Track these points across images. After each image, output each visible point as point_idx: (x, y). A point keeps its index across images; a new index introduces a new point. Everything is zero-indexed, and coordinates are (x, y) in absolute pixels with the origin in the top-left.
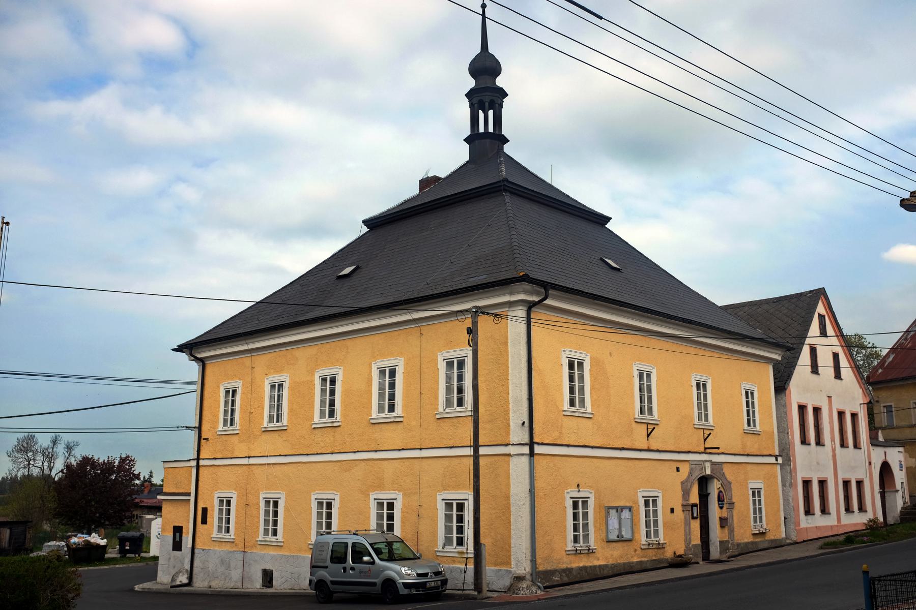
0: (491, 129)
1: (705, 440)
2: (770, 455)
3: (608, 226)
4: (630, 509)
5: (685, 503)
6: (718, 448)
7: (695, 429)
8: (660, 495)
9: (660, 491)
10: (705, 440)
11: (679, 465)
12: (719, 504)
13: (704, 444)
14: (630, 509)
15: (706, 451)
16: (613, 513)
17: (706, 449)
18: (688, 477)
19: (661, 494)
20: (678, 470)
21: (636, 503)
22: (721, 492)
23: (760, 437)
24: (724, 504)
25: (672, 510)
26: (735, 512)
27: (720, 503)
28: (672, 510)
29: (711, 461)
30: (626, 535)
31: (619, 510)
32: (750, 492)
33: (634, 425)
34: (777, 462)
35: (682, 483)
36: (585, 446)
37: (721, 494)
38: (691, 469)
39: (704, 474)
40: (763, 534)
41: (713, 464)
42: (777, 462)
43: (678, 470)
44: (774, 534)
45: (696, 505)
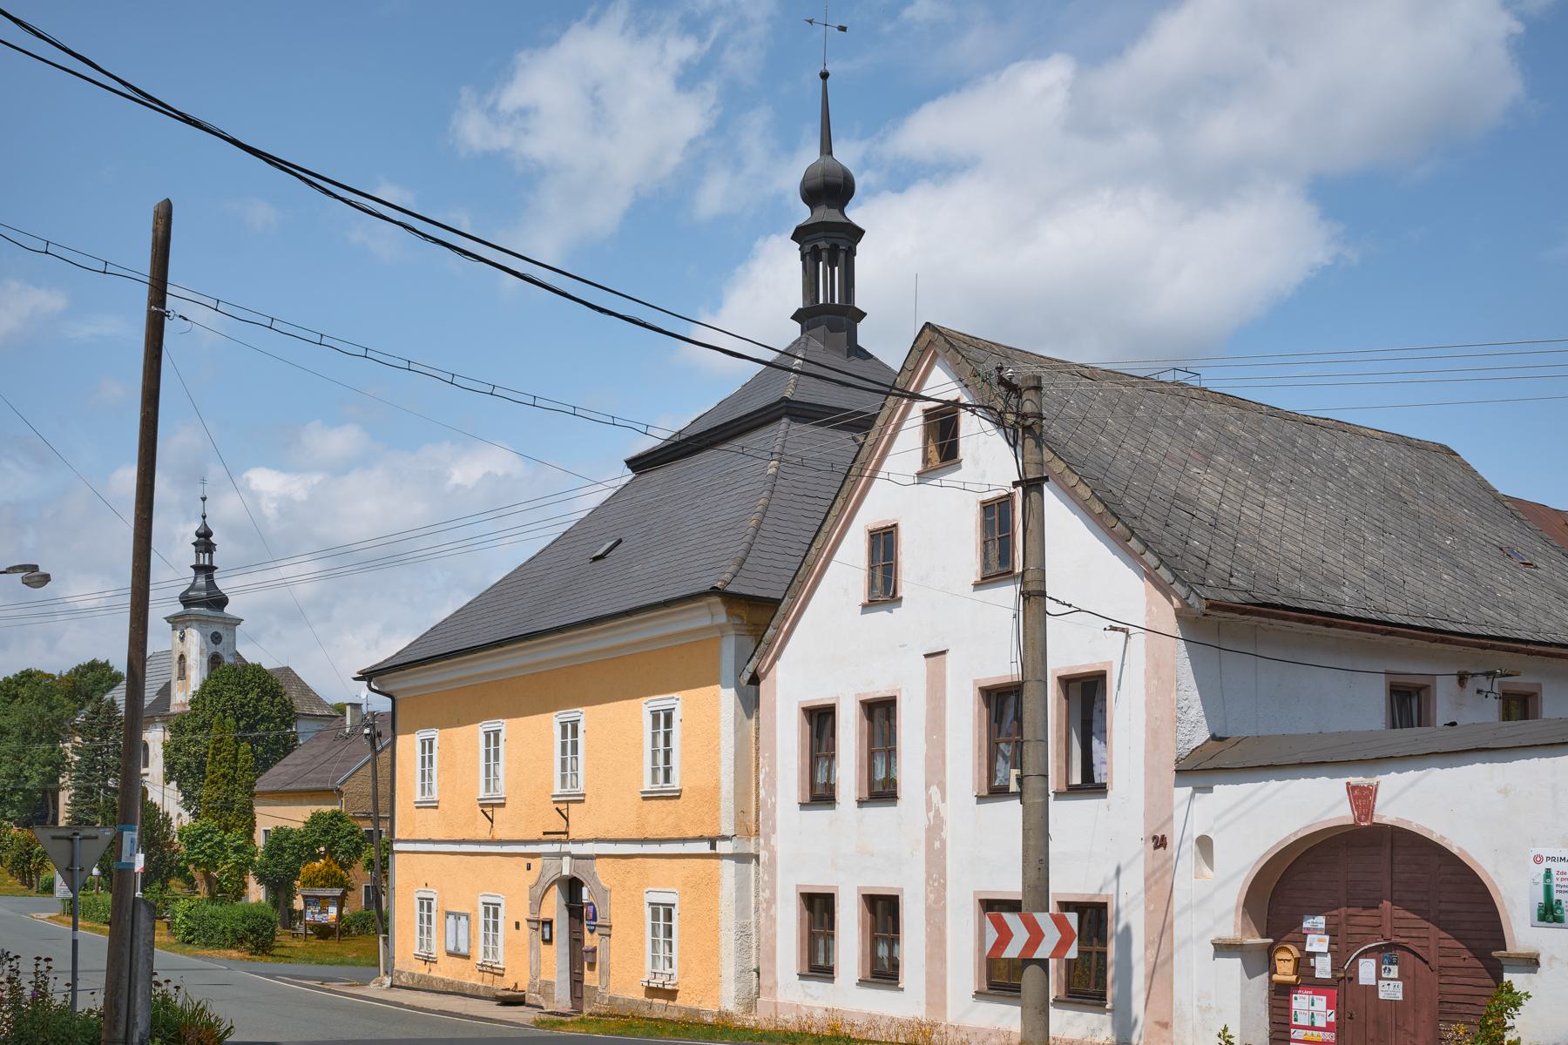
2: (701, 839)
4: (468, 917)
5: (531, 917)
8: (503, 903)
11: (530, 860)
14: (468, 917)
15: (563, 836)
16: (451, 918)
19: (503, 901)
20: (529, 868)
21: (476, 910)
23: (679, 802)
25: (517, 925)
28: (517, 925)
29: (568, 854)
30: (464, 949)
31: (457, 916)
32: (648, 911)
34: (713, 851)
35: (531, 888)
40: (671, 994)
42: (713, 851)
43: (529, 868)
44: (699, 1000)
45: (550, 923)
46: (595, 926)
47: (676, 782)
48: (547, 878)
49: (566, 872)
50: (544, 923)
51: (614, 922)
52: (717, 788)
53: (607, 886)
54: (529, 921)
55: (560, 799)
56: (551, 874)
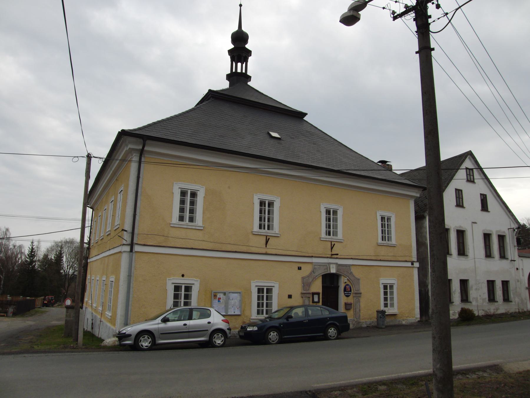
0: (244, 71)
1: (332, 248)
3: (305, 118)
6: (337, 254)
7: (322, 242)
9: (277, 283)
10: (332, 248)
12: (345, 294)
13: (331, 251)
17: (332, 255)
18: (311, 274)
22: (347, 285)
24: (350, 294)
25: (290, 297)
26: (362, 300)
27: (346, 292)
28: (290, 297)
29: (336, 264)
32: (382, 287)
33: (251, 236)
36: (192, 249)
37: (347, 286)
38: (315, 268)
39: (329, 272)
41: (338, 265)
42: (413, 266)
43: (300, 268)
44: (407, 315)
45: (318, 294)
46: (350, 294)
47: (393, 242)
48: (316, 274)
49: (333, 271)
50: (313, 294)
51: (362, 291)
52: (411, 246)
53: (359, 278)
54: (301, 293)
55: (327, 240)
56: (322, 271)
